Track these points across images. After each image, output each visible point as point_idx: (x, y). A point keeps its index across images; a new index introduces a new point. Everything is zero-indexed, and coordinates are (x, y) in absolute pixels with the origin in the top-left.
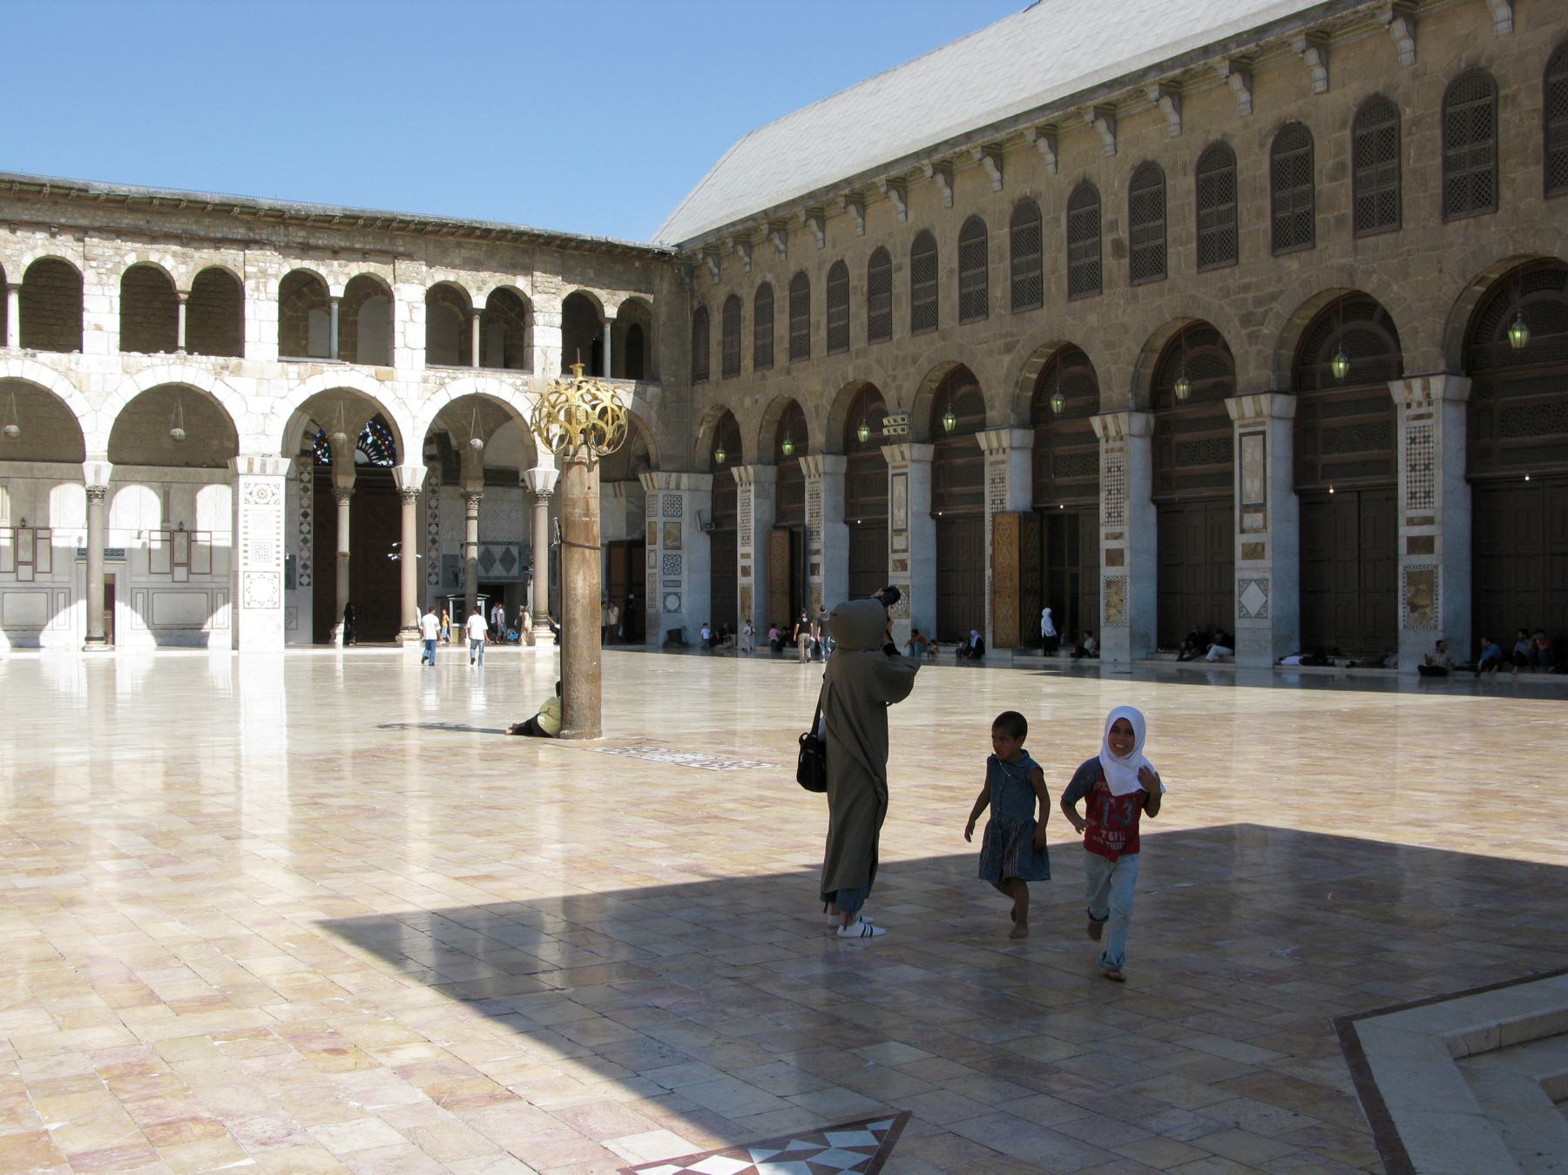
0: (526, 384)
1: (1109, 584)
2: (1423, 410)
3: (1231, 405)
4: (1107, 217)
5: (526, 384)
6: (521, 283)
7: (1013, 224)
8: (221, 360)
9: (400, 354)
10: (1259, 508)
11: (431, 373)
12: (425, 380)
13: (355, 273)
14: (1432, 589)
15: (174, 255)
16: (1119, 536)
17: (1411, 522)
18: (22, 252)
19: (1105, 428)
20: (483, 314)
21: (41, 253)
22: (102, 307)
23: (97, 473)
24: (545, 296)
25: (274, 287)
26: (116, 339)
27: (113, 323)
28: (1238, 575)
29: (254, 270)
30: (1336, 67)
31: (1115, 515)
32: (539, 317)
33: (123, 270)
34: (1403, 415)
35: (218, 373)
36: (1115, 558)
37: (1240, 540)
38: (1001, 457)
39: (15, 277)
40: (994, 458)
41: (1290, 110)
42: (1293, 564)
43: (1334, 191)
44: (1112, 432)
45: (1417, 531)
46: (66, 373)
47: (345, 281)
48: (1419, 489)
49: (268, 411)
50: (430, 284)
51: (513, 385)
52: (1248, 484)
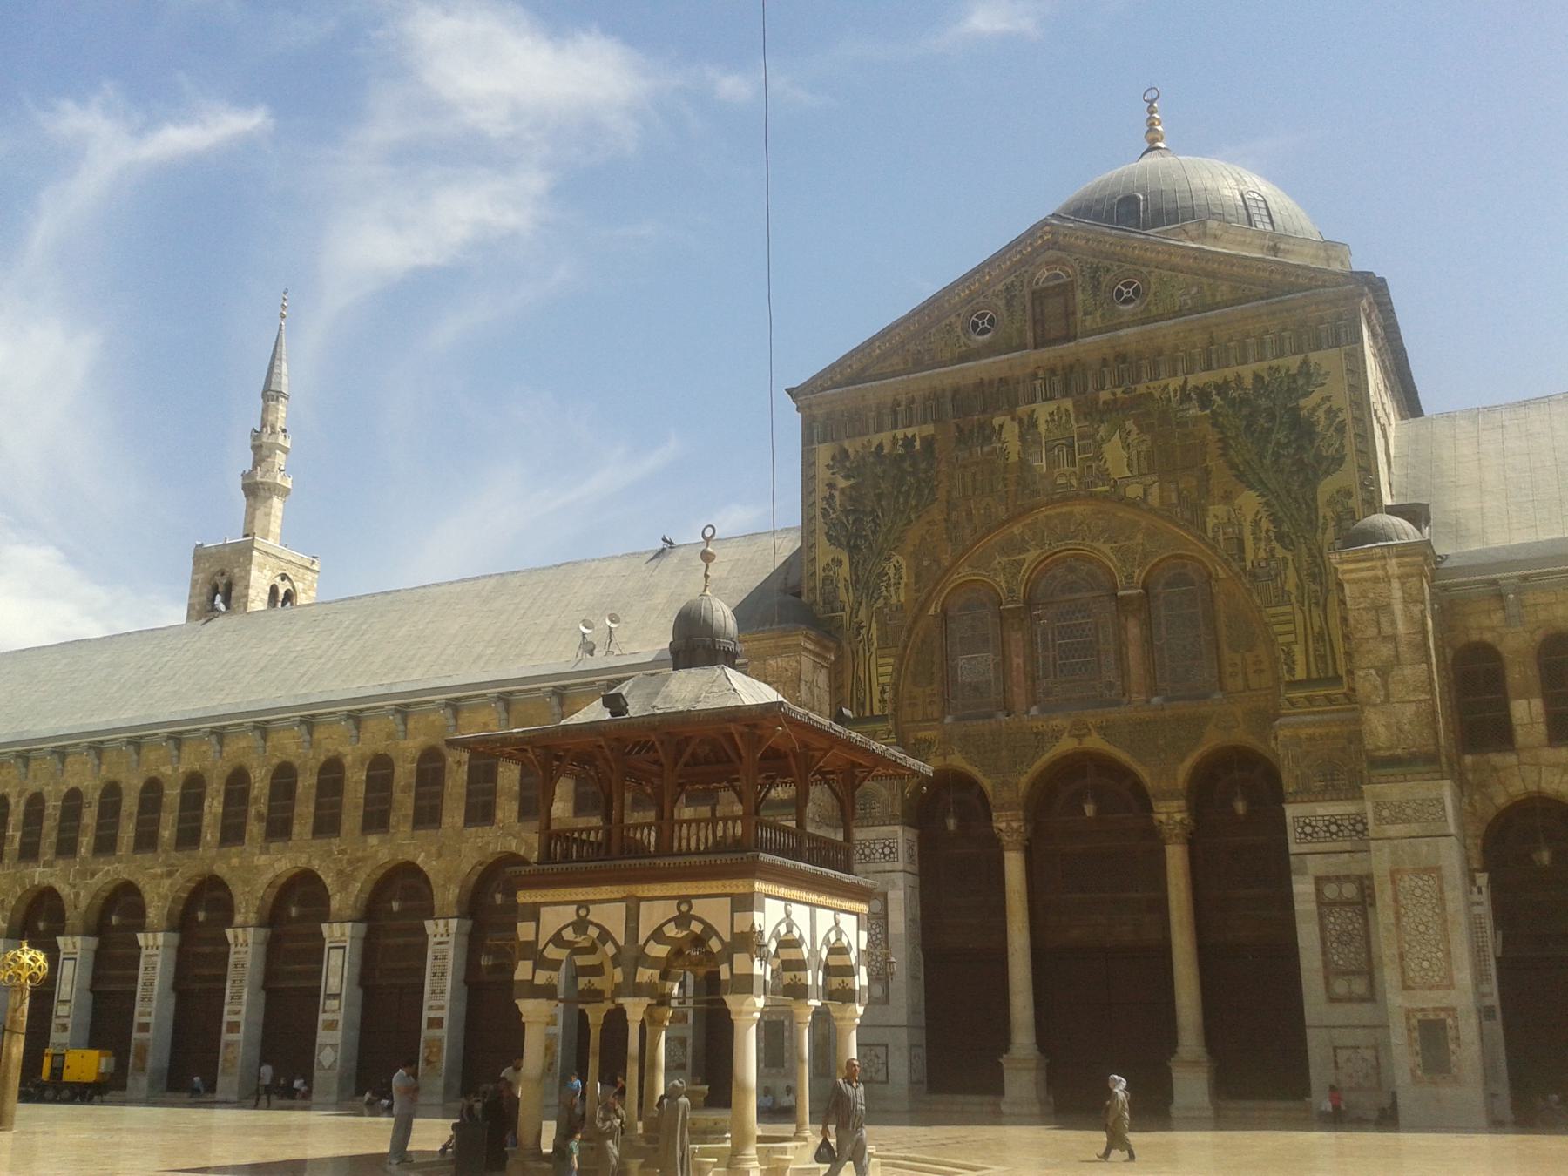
1: (228, 1045)
2: (445, 939)
3: (325, 927)
4: (254, 793)
7: (183, 788)
10: (336, 996)
14: (440, 1050)
16: (237, 1013)
17: (431, 1008)
19: (236, 937)
28: (318, 1041)
30: (411, 725)
31: (237, 997)
34: (432, 941)
36: (234, 1027)
37: (322, 1017)
38: (154, 952)
40: (150, 952)
41: (381, 746)
42: (355, 1035)
43: (404, 802)
44: (241, 940)
45: (433, 1014)
48: (437, 988)
52: (331, 980)
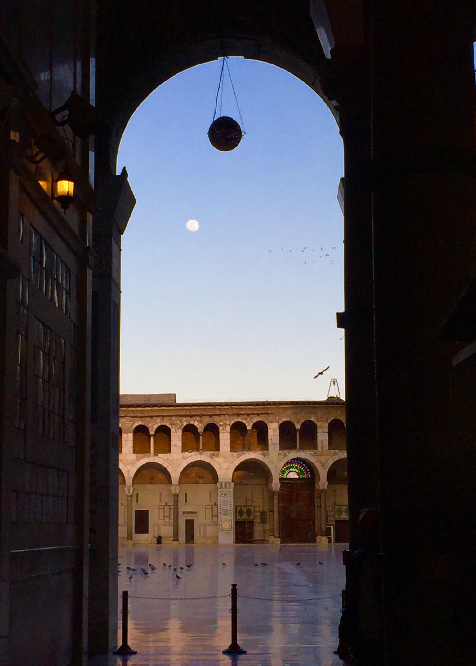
0: (315, 453)
5: (315, 453)
6: (313, 419)
8: (212, 452)
9: (270, 446)
11: (281, 452)
12: (279, 454)
13: (255, 421)
15: (198, 421)
18: (154, 425)
20: (301, 430)
21: (159, 425)
22: (177, 438)
23: (175, 490)
24: (321, 423)
25: (228, 428)
26: (181, 449)
27: (180, 443)
29: (222, 423)
32: (319, 430)
33: (183, 427)
35: (212, 456)
39: (152, 432)
46: (167, 460)
47: (252, 424)
49: (227, 467)
50: (280, 422)
51: (310, 454)
